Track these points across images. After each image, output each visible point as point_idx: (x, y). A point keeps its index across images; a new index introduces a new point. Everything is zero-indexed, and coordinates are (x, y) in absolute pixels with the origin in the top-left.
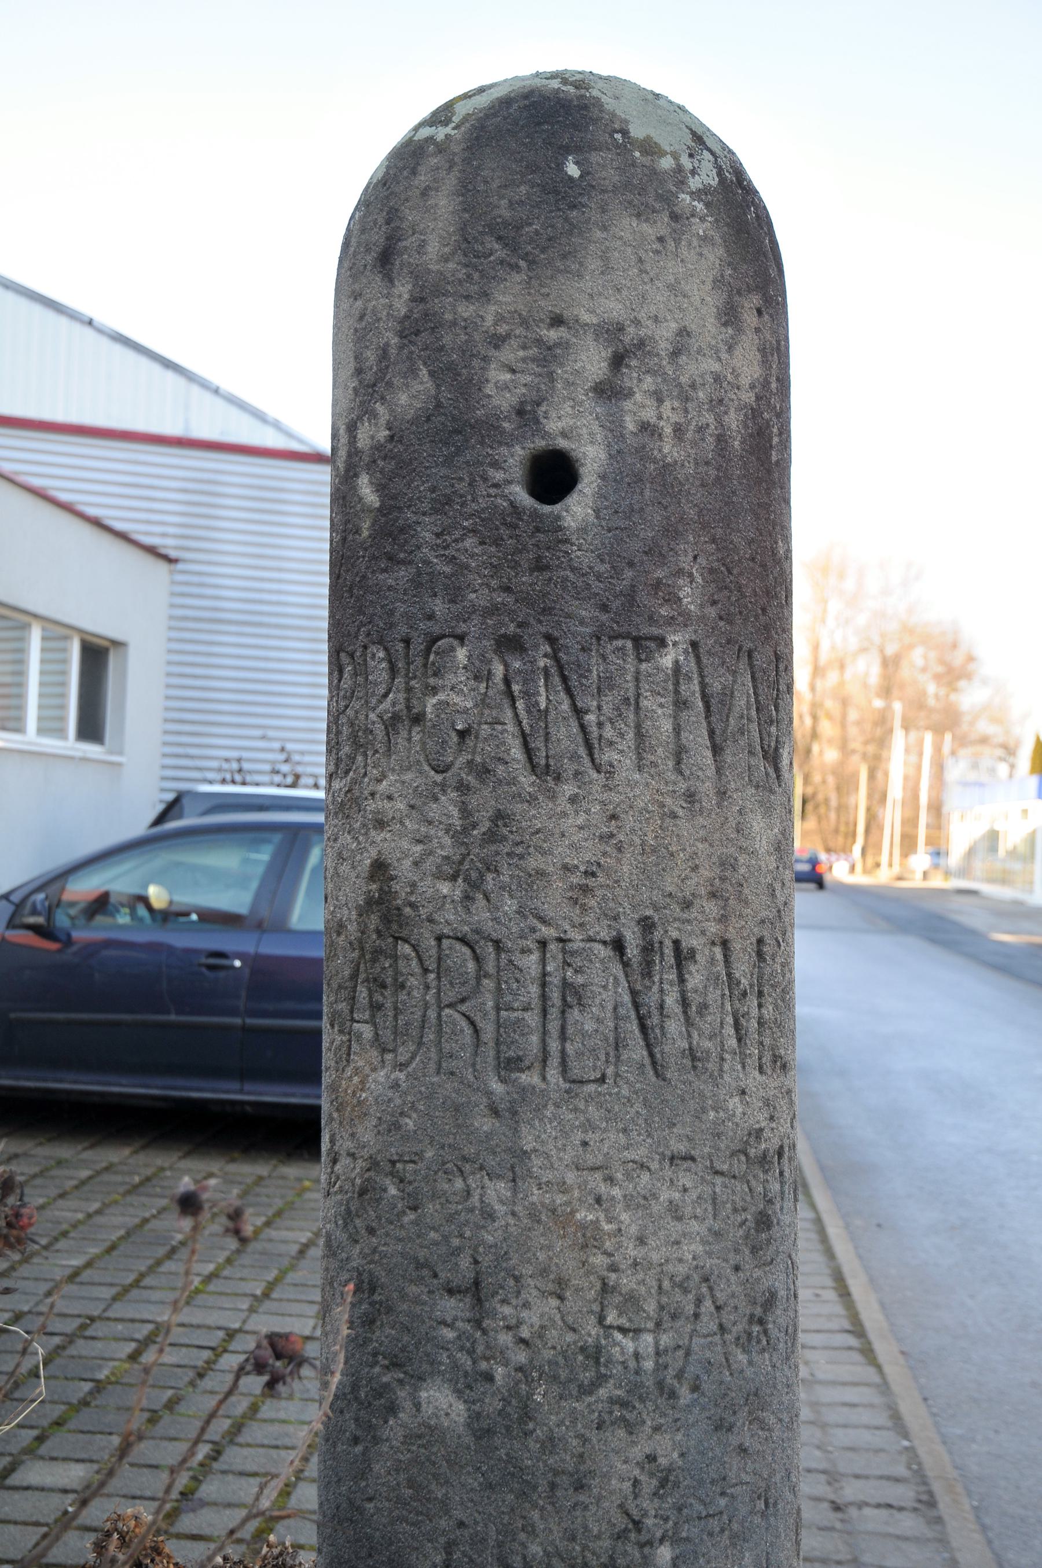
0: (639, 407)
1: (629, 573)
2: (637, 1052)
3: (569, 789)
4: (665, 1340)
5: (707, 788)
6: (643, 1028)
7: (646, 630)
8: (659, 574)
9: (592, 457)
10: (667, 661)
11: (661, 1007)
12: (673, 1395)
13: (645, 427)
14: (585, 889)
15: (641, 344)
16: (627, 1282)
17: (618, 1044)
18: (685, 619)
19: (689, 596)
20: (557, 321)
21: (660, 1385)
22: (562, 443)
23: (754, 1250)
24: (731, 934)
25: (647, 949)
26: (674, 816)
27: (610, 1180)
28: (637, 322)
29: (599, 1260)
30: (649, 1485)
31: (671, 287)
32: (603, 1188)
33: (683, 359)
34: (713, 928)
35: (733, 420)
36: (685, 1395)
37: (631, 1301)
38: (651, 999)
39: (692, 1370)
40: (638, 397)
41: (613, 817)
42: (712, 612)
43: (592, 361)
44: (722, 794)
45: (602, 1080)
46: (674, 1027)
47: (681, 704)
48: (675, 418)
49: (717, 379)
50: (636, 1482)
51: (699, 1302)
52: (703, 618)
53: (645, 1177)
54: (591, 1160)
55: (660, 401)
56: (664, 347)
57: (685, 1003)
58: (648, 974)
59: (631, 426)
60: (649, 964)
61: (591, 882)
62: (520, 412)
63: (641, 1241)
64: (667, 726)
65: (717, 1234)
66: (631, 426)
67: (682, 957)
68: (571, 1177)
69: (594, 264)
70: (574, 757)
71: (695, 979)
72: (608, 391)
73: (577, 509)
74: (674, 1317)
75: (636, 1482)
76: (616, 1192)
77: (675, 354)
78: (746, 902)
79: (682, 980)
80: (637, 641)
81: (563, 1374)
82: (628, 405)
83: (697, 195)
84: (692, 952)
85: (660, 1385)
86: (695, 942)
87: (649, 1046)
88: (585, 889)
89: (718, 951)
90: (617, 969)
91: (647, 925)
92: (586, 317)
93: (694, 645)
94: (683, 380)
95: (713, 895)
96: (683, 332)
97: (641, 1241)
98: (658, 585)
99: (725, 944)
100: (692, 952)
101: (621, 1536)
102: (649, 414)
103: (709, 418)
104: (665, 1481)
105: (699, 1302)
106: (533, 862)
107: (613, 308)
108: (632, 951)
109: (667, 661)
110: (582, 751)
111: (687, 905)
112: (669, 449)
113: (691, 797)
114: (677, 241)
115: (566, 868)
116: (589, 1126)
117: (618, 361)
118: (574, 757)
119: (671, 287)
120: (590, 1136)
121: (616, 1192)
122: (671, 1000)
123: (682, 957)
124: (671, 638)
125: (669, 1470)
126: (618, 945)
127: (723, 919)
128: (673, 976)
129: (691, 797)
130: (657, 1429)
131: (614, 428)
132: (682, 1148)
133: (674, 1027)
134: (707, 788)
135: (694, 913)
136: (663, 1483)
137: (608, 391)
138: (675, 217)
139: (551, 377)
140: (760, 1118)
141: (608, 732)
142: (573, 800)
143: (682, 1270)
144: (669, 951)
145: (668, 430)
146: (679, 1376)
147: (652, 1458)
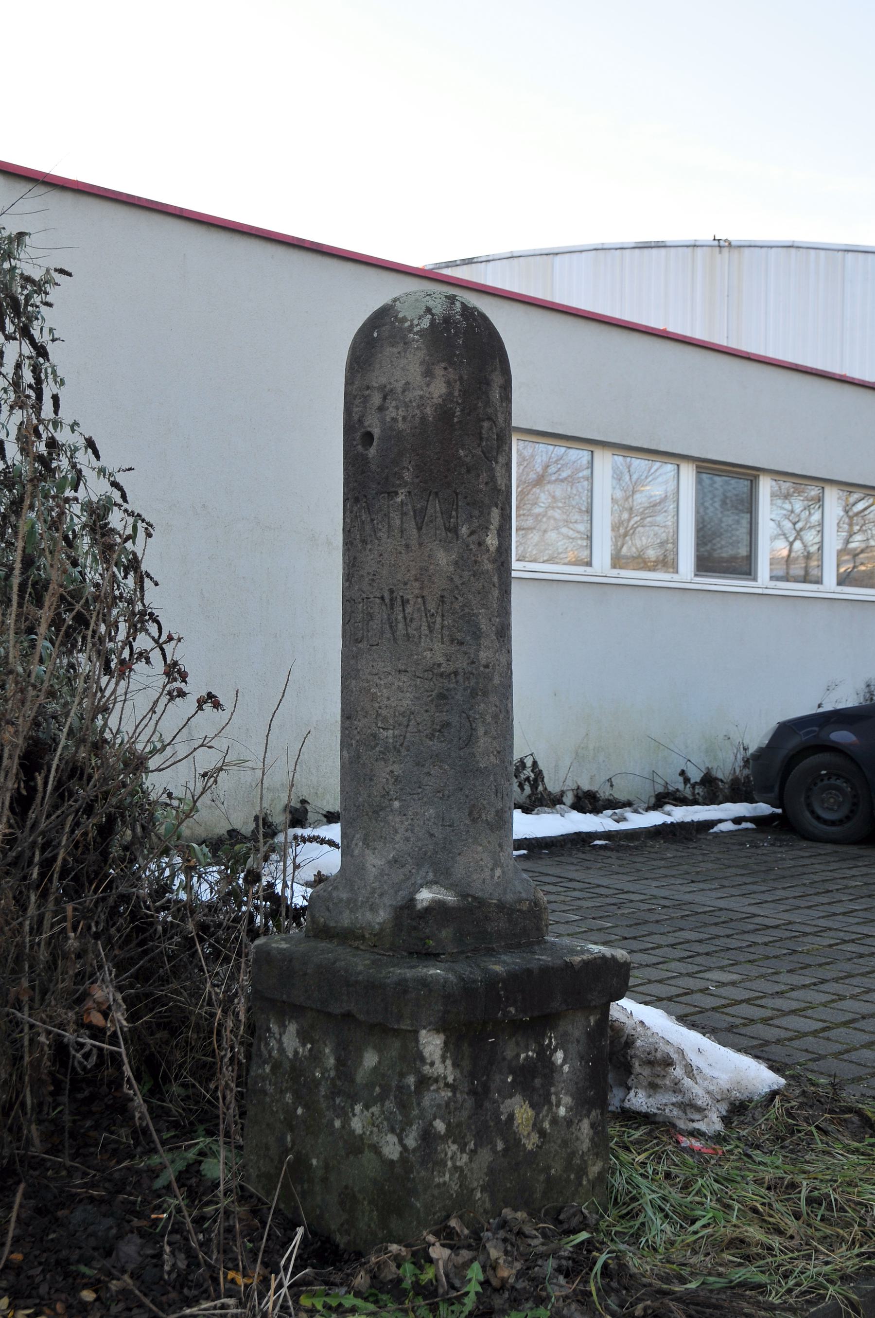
0: (391, 413)
1: (387, 471)
2: (389, 635)
3: (369, 546)
4: (396, 732)
5: (414, 543)
6: (391, 627)
7: (392, 489)
8: (396, 469)
9: (376, 432)
10: (399, 500)
11: (396, 619)
12: (399, 751)
13: (393, 419)
14: (373, 580)
15: (392, 390)
16: (384, 712)
17: (382, 632)
18: (406, 484)
19: (407, 476)
20: (368, 388)
21: (395, 747)
22: (369, 429)
23: (437, 706)
24: (425, 593)
25: (391, 600)
26: (400, 553)
27: (380, 678)
28: (390, 383)
29: (376, 705)
30: (391, 780)
31: (402, 369)
32: (378, 681)
33: (407, 393)
34: (417, 592)
35: (428, 411)
36: (404, 752)
37: (385, 719)
38: (393, 617)
39: (406, 744)
40: (391, 409)
41: (381, 555)
42: (417, 480)
43: (376, 400)
44: (421, 544)
45: (377, 645)
46: (401, 626)
47: (404, 514)
48: (403, 414)
49: (421, 397)
50: (387, 779)
51: (409, 721)
52: (413, 483)
53: (390, 677)
54: (375, 671)
55: (398, 409)
56: (399, 390)
57: (405, 618)
58: (392, 608)
59: (388, 419)
60: (392, 605)
61: (375, 578)
62: (359, 421)
63: (388, 699)
64: (398, 522)
65: (418, 698)
66: (388, 419)
67: (404, 602)
68: (369, 677)
69: (378, 366)
70: (371, 535)
71: (409, 609)
72: (381, 409)
73: (372, 451)
74: (400, 725)
75: (387, 779)
76: (382, 682)
77: (404, 391)
78: (433, 583)
79: (404, 610)
80: (389, 493)
81: (367, 743)
82: (387, 412)
83: (416, 333)
84: (408, 601)
85: (395, 747)
86: (409, 597)
87: (393, 634)
88: (373, 580)
89: (419, 600)
90: (384, 608)
91: (391, 591)
92: (375, 385)
93: (409, 492)
94: (407, 400)
95: (416, 580)
96: (407, 383)
97: (388, 699)
98: (396, 473)
99: (423, 597)
100: (408, 601)
101: (383, 796)
102: (394, 415)
103: (418, 412)
104: (397, 780)
105: (409, 721)
106: (361, 573)
107: (383, 380)
108: (387, 601)
109: (399, 500)
110: (372, 534)
111: (406, 584)
112: (401, 425)
113: (407, 546)
114: (405, 352)
115: (369, 573)
116: (374, 660)
117: (385, 398)
118: (371, 535)
119: (402, 369)
120: (375, 664)
121: (382, 682)
122: (400, 617)
123: (404, 602)
124: (400, 491)
125: (398, 777)
126: (382, 598)
127: (421, 588)
128: (401, 609)
129: (407, 546)
130: (394, 762)
131: (383, 421)
132: (403, 668)
133: (401, 626)
134: (414, 543)
135: (408, 587)
136: (396, 780)
137: (381, 409)
138: (405, 343)
139: (365, 407)
140: (441, 660)
141: (380, 526)
142: (370, 550)
143: (402, 709)
144: (399, 600)
145: (400, 419)
146: (402, 745)
147: (392, 772)
